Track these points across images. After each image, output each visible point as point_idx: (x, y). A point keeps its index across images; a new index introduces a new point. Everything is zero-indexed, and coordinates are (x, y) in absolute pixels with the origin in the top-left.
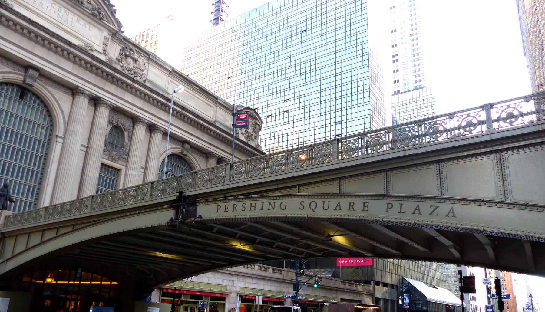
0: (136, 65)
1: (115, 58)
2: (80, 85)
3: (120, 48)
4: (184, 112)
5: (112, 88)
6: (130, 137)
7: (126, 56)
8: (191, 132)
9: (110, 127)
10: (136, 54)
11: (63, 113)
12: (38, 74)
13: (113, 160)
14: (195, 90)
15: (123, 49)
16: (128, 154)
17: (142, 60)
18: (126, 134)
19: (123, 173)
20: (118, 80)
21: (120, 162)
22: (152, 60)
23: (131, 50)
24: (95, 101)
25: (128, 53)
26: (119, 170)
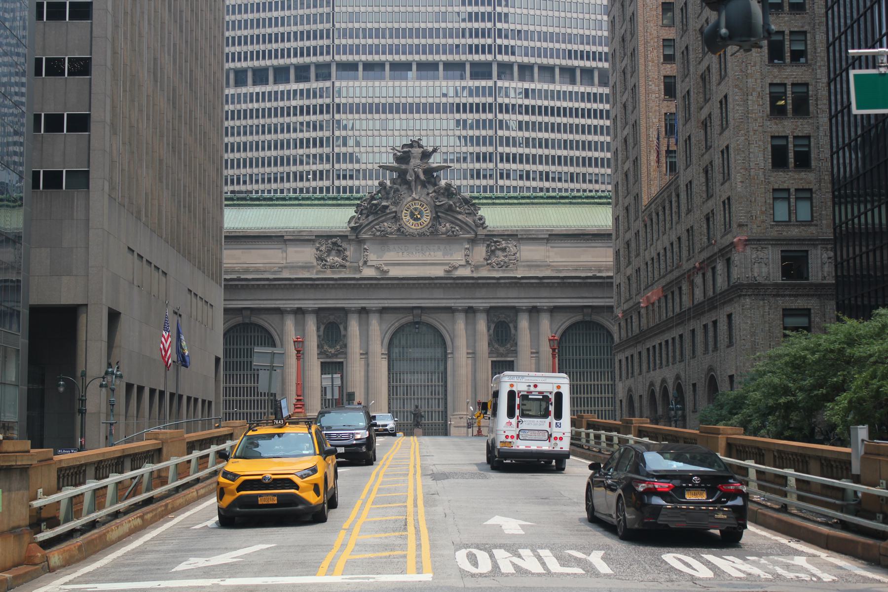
0: (505, 254)
1: (482, 260)
2: (453, 305)
3: (485, 245)
4: (565, 281)
5: (483, 292)
6: (516, 328)
7: (493, 252)
8: (587, 295)
9: (493, 326)
10: (503, 242)
11: (447, 331)
12: (420, 311)
13: (502, 355)
14: (588, 240)
15: (488, 246)
16: (516, 344)
17: (511, 246)
18: (511, 325)
19: (515, 364)
20: (483, 284)
21: (510, 355)
22: (522, 239)
23: (497, 242)
24: (470, 311)
25: (493, 248)
26: (513, 361)
